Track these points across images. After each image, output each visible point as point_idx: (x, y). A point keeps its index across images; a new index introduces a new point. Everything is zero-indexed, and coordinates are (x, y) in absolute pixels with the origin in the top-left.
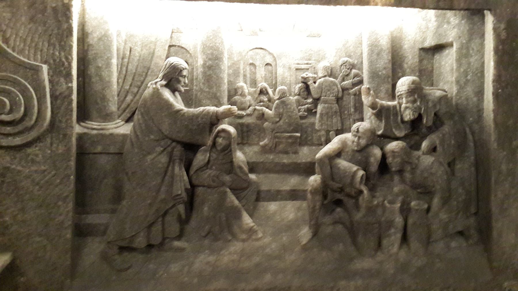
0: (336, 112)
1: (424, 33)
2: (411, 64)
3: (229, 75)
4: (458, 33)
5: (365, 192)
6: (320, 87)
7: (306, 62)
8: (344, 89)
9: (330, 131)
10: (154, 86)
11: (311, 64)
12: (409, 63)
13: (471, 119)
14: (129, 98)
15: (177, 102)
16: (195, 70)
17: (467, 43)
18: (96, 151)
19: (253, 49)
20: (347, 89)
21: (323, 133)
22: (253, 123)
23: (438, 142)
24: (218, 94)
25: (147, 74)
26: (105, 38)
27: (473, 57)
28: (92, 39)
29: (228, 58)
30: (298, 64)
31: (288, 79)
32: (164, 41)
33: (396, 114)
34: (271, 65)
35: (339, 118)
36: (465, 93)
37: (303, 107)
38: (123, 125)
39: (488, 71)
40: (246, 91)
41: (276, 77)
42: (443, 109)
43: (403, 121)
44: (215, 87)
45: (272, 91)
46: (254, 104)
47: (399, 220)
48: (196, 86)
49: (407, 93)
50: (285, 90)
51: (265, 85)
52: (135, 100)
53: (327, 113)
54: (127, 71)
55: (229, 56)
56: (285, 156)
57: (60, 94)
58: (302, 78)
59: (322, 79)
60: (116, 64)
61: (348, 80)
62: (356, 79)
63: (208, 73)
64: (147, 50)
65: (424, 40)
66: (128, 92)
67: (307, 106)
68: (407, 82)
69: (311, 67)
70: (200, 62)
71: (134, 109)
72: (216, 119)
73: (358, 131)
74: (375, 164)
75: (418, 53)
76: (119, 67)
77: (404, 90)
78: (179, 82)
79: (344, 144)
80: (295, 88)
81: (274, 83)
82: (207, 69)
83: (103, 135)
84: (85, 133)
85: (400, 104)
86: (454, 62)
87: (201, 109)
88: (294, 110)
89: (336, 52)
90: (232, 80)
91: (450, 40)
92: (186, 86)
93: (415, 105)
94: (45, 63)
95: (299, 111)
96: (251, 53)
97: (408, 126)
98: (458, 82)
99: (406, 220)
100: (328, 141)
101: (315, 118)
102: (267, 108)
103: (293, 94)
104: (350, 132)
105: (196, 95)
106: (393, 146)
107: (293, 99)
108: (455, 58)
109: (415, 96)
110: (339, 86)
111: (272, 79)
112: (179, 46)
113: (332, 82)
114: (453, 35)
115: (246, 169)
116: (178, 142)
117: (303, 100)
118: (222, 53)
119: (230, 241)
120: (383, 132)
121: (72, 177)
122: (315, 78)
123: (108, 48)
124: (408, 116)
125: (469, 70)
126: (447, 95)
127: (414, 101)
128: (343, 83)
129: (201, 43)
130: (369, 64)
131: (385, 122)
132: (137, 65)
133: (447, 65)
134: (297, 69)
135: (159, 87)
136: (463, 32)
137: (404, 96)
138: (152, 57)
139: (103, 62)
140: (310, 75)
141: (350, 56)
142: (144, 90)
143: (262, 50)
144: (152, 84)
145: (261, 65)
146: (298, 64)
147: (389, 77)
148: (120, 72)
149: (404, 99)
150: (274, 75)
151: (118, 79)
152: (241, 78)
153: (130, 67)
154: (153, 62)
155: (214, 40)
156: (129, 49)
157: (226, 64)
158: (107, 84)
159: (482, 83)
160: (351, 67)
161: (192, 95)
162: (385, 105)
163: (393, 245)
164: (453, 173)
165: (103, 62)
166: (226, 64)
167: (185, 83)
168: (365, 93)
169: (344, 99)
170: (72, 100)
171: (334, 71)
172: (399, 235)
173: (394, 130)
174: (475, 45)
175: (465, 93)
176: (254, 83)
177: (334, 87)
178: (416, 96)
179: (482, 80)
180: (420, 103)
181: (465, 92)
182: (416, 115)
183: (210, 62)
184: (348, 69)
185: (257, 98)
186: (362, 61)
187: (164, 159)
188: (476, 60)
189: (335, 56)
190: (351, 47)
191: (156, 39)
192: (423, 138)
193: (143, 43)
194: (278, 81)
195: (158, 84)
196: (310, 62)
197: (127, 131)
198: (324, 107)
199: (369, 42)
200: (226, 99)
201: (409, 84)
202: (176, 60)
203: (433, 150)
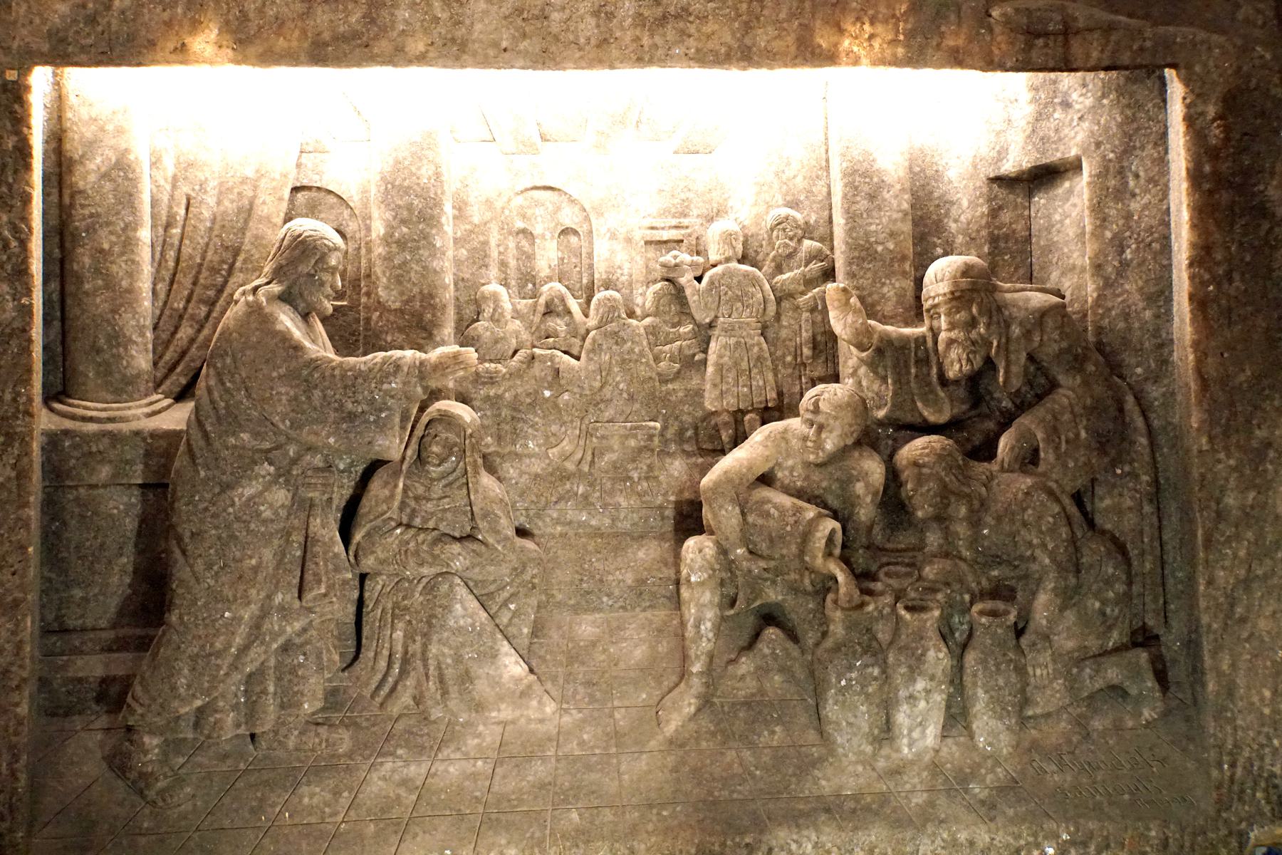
0: (759, 359)
1: (998, 134)
2: (968, 224)
3: (458, 263)
4: (1092, 132)
5: (841, 578)
7: (674, 222)
8: (782, 297)
10: (251, 298)
12: (963, 218)
13: (1139, 370)
14: (185, 332)
15: (313, 341)
16: (363, 251)
17: (1120, 159)
18: (94, 480)
19: (527, 190)
20: (791, 295)
22: (529, 395)
23: (1040, 435)
25: (232, 266)
26: (121, 170)
27: (1138, 198)
28: (87, 176)
29: (455, 218)
30: (652, 228)
31: (626, 271)
32: (278, 177)
33: (923, 361)
34: (575, 232)
35: (770, 376)
36: (1120, 299)
37: (667, 348)
38: (169, 407)
39: (1179, 236)
40: (507, 306)
41: (591, 266)
43: (943, 381)
45: (580, 304)
48: (368, 294)
49: (951, 300)
50: (615, 300)
52: (201, 337)
54: (177, 261)
55: (456, 212)
58: (664, 265)
60: (148, 241)
61: (791, 270)
64: (232, 201)
65: (1002, 154)
66: (181, 317)
67: (678, 343)
69: (690, 235)
70: (378, 229)
73: (816, 410)
74: (868, 499)
75: (985, 190)
77: (942, 292)
81: (585, 281)
82: (394, 248)
83: (115, 438)
85: (935, 333)
86: (1087, 212)
87: (380, 355)
88: (642, 354)
90: (467, 276)
91: (1074, 152)
93: (974, 335)
95: (657, 359)
96: (519, 201)
97: (961, 392)
98: (1098, 268)
100: (739, 438)
101: (703, 379)
102: (565, 352)
103: (638, 311)
104: (797, 415)
105: (368, 320)
106: (917, 448)
108: (1087, 203)
109: (970, 309)
111: (580, 273)
112: (319, 189)
113: (746, 275)
114: (1080, 137)
118: (438, 204)
120: (891, 411)
123: (127, 199)
124: (956, 364)
126: (1064, 306)
127: (973, 323)
129: (378, 178)
130: (846, 224)
131: (895, 383)
132: (207, 245)
133: (1067, 221)
134: (648, 243)
135: (264, 299)
137: (942, 310)
138: (246, 221)
139: (113, 238)
140: (685, 257)
141: (794, 204)
142: (223, 312)
143: (549, 193)
144: (244, 293)
145: (548, 235)
146: (652, 228)
147: (904, 258)
148: (160, 264)
149: (943, 317)
150: (585, 261)
151: (155, 284)
152: (494, 272)
153: (186, 250)
154: (248, 234)
155: (413, 169)
156: (184, 201)
157: (450, 233)
158: (124, 298)
159: (1168, 268)
161: (358, 321)
162: (894, 335)
165: (113, 238)
168: (836, 304)
172: (939, 698)
173: (919, 404)
175: (1120, 299)
176: (527, 281)
178: (974, 310)
179: (1165, 262)
180: (988, 326)
181: (1118, 296)
182: (978, 362)
183: (405, 230)
184: (791, 239)
188: (1145, 207)
191: (257, 171)
192: (1004, 426)
193: (221, 184)
194: (596, 276)
195: (261, 291)
196: (685, 222)
197: (178, 423)
198: (725, 346)
199: (845, 165)
200: (448, 330)
201: (955, 277)
203: (1029, 459)
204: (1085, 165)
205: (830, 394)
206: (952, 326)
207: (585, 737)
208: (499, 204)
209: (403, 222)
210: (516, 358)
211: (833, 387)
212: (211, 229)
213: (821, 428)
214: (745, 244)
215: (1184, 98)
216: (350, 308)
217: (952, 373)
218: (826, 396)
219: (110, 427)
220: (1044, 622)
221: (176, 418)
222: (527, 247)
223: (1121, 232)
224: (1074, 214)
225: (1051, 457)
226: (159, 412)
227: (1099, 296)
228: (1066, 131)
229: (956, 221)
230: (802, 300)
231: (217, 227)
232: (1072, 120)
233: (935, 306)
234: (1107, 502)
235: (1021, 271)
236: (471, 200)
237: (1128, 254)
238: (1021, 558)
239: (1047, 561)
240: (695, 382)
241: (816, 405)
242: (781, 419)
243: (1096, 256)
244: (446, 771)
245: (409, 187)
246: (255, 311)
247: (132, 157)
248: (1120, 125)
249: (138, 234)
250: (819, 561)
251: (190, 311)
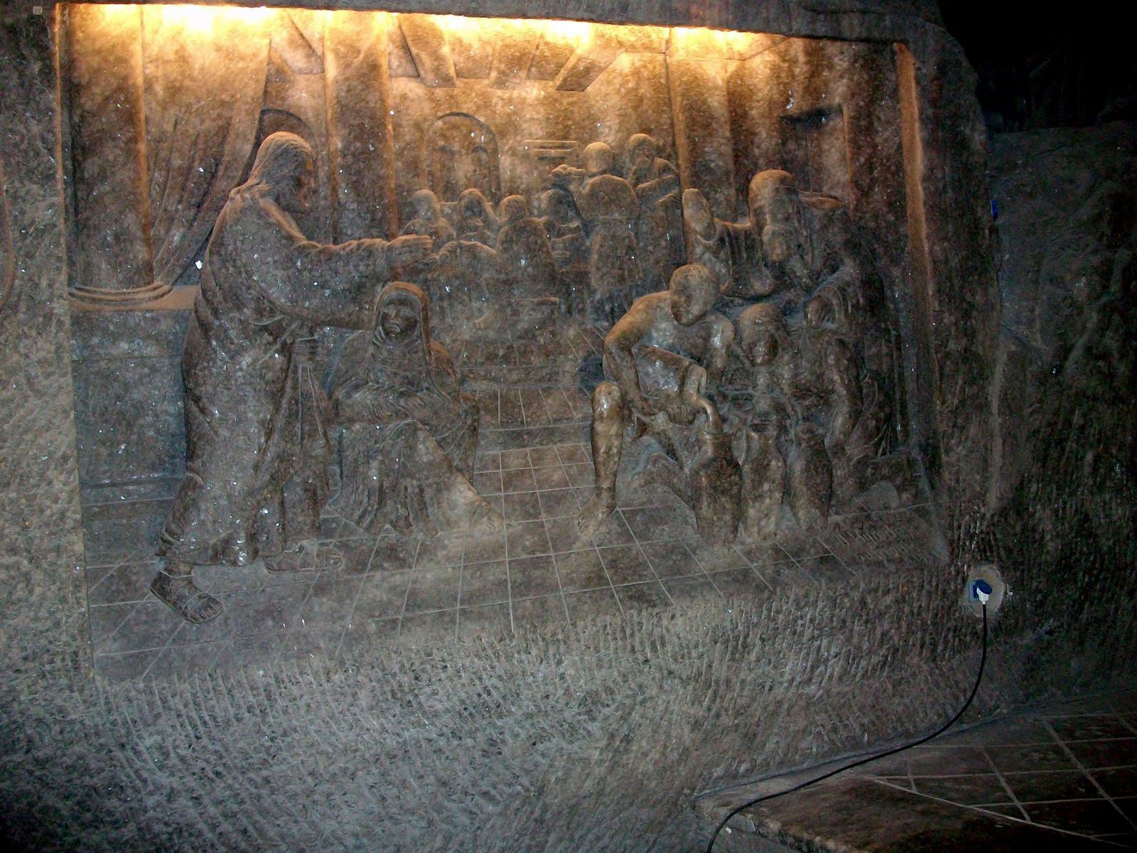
2: (768, 150)
5: (709, 411)
11: (567, 148)
51: (477, 191)
58: (557, 175)
69: (570, 154)
80: (539, 199)
82: (350, 159)
85: (760, 226)
86: (847, 144)
89: (621, 124)
91: (837, 100)
98: (856, 184)
103: (536, 212)
113: (618, 183)
133: (833, 150)
136: (858, 84)
141: (648, 131)
156: (173, 120)
172: (778, 495)
176: (449, 190)
183: (358, 144)
188: (886, 140)
189: (618, 132)
204: (845, 109)
207: (527, 543)
208: (425, 126)
220: (842, 436)
223: (871, 157)
226: (163, 295)
229: (758, 147)
232: (835, 77)
233: (761, 207)
234: (874, 350)
236: (404, 123)
237: (876, 173)
239: (845, 392)
244: (424, 577)
250: (695, 398)
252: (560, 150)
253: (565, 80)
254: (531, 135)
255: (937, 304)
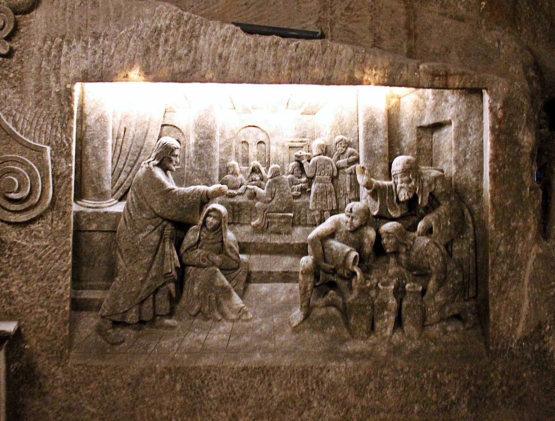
0: (331, 192)
1: (421, 111)
2: (409, 143)
3: (221, 153)
5: (358, 274)
6: (315, 164)
7: (300, 140)
9: (324, 211)
13: (471, 200)
14: (123, 176)
15: (169, 181)
16: (186, 148)
17: (465, 121)
18: (91, 229)
20: (343, 168)
21: (317, 212)
22: (245, 203)
23: (433, 223)
24: (210, 173)
25: (140, 153)
26: (101, 119)
28: (90, 121)
29: (220, 137)
32: (157, 121)
34: (264, 143)
35: (334, 198)
37: (296, 186)
38: (116, 203)
39: (486, 151)
40: (238, 170)
41: (269, 156)
42: (439, 188)
44: (206, 166)
46: (246, 184)
47: (392, 302)
48: (188, 164)
49: (402, 172)
51: (257, 163)
53: (321, 193)
56: (277, 236)
57: (61, 173)
58: (296, 156)
59: (317, 157)
61: (343, 159)
62: (351, 158)
63: (200, 152)
66: (121, 171)
67: (300, 185)
68: (401, 162)
70: (192, 141)
71: (127, 188)
72: (207, 198)
74: (369, 245)
75: (416, 131)
76: (114, 146)
77: (399, 169)
78: (171, 161)
79: (338, 224)
81: (267, 161)
82: (198, 148)
84: (81, 211)
86: (453, 141)
87: (192, 188)
88: (287, 188)
89: (332, 130)
90: (224, 158)
91: (448, 118)
92: (178, 165)
93: (410, 185)
94: (48, 144)
97: (405, 206)
98: (456, 161)
99: (400, 303)
100: (322, 221)
101: (309, 198)
102: (259, 187)
103: (286, 172)
105: (187, 174)
106: (388, 226)
107: (287, 177)
108: (453, 137)
110: (334, 165)
112: (171, 125)
113: (326, 160)
114: (451, 113)
115: (237, 249)
116: (169, 221)
117: (297, 179)
118: (214, 132)
119: (219, 321)
120: (378, 212)
121: (70, 253)
122: (309, 156)
123: (104, 129)
124: (403, 195)
125: (468, 149)
126: (444, 176)
127: (409, 181)
128: (338, 161)
131: (380, 202)
132: (131, 145)
135: (152, 166)
136: (461, 110)
137: (399, 176)
138: (145, 137)
139: (99, 143)
140: (304, 153)
141: (345, 134)
143: (255, 128)
145: (254, 143)
147: (385, 156)
148: (114, 152)
150: (267, 154)
151: (112, 159)
152: (233, 156)
155: (206, 119)
157: (218, 143)
158: (101, 163)
159: (482, 163)
160: (347, 145)
161: (184, 174)
163: (386, 327)
164: (450, 254)
166: (218, 141)
167: (176, 162)
169: (340, 178)
170: (71, 179)
171: (329, 148)
172: (392, 318)
173: (389, 210)
174: (473, 124)
176: (246, 161)
177: (328, 166)
180: (415, 183)
182: (411, 195)
183: (202, 141)
185: (249, 177)
186: (358, 139)
187: (155, 237)
188: (475, 139)
189: (331, 134)
190: (347, 125)
192: (420, 219)
193: (136, 123)
196: (304, 140)
197: (120, 209)
198: (318, 186)
199: (364, 121)
200: (217, 178)
202: (169, 140)
203: (428, 231)
205: (356, 206)
206: (402, 182)
209: (202, 138)
210: (241, 188)
211: (358, 203)
212: (133, 139)
213: (352, 218)
214: (326, 149)
215: (489, 101)
216: (181, 169)
217: (402, 199)
218: (355, 206)
219: (96, 210)
221: (120, 207)
222: (246, 148)
224: (448, 141)
225: (437, 231)
226: (113, 205)
227: (456, 172)
228: (446, 110)
229: (405, 142)
230: (347, 170)
231: (135, 139)
233: (396, 174)
235: (428, 161)
236: (226, 130)
237: (468, 157)
238: (424, 268)
240: (307, 199)
241: (351, 209)
242: (338, 213)
243: (456, 157)
245: (204, 126)
246: (149, 170)
247: (106, 114)
248: (466, 109)
249: (108, 141)
251: (124, 169)
252: (300, 143)
253: (305, 110)
254: (287, 135)
255: (493, 226)
